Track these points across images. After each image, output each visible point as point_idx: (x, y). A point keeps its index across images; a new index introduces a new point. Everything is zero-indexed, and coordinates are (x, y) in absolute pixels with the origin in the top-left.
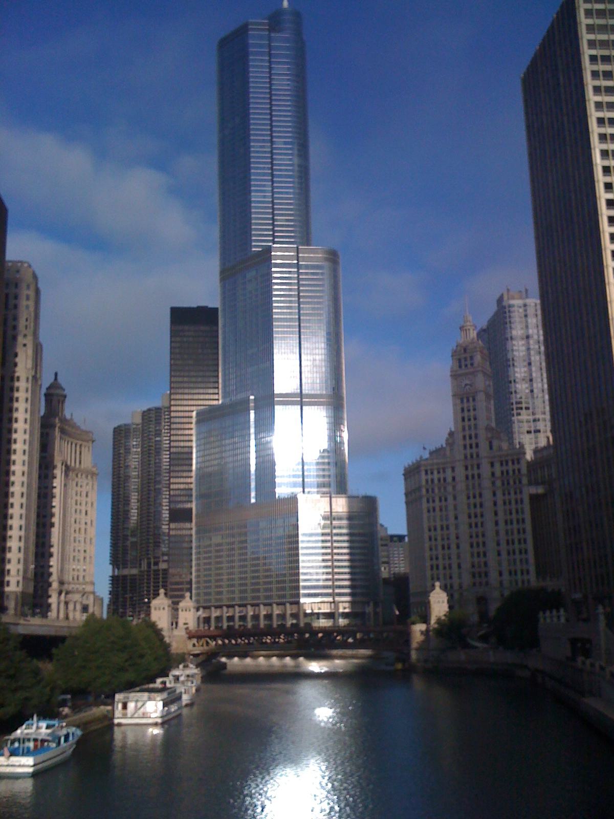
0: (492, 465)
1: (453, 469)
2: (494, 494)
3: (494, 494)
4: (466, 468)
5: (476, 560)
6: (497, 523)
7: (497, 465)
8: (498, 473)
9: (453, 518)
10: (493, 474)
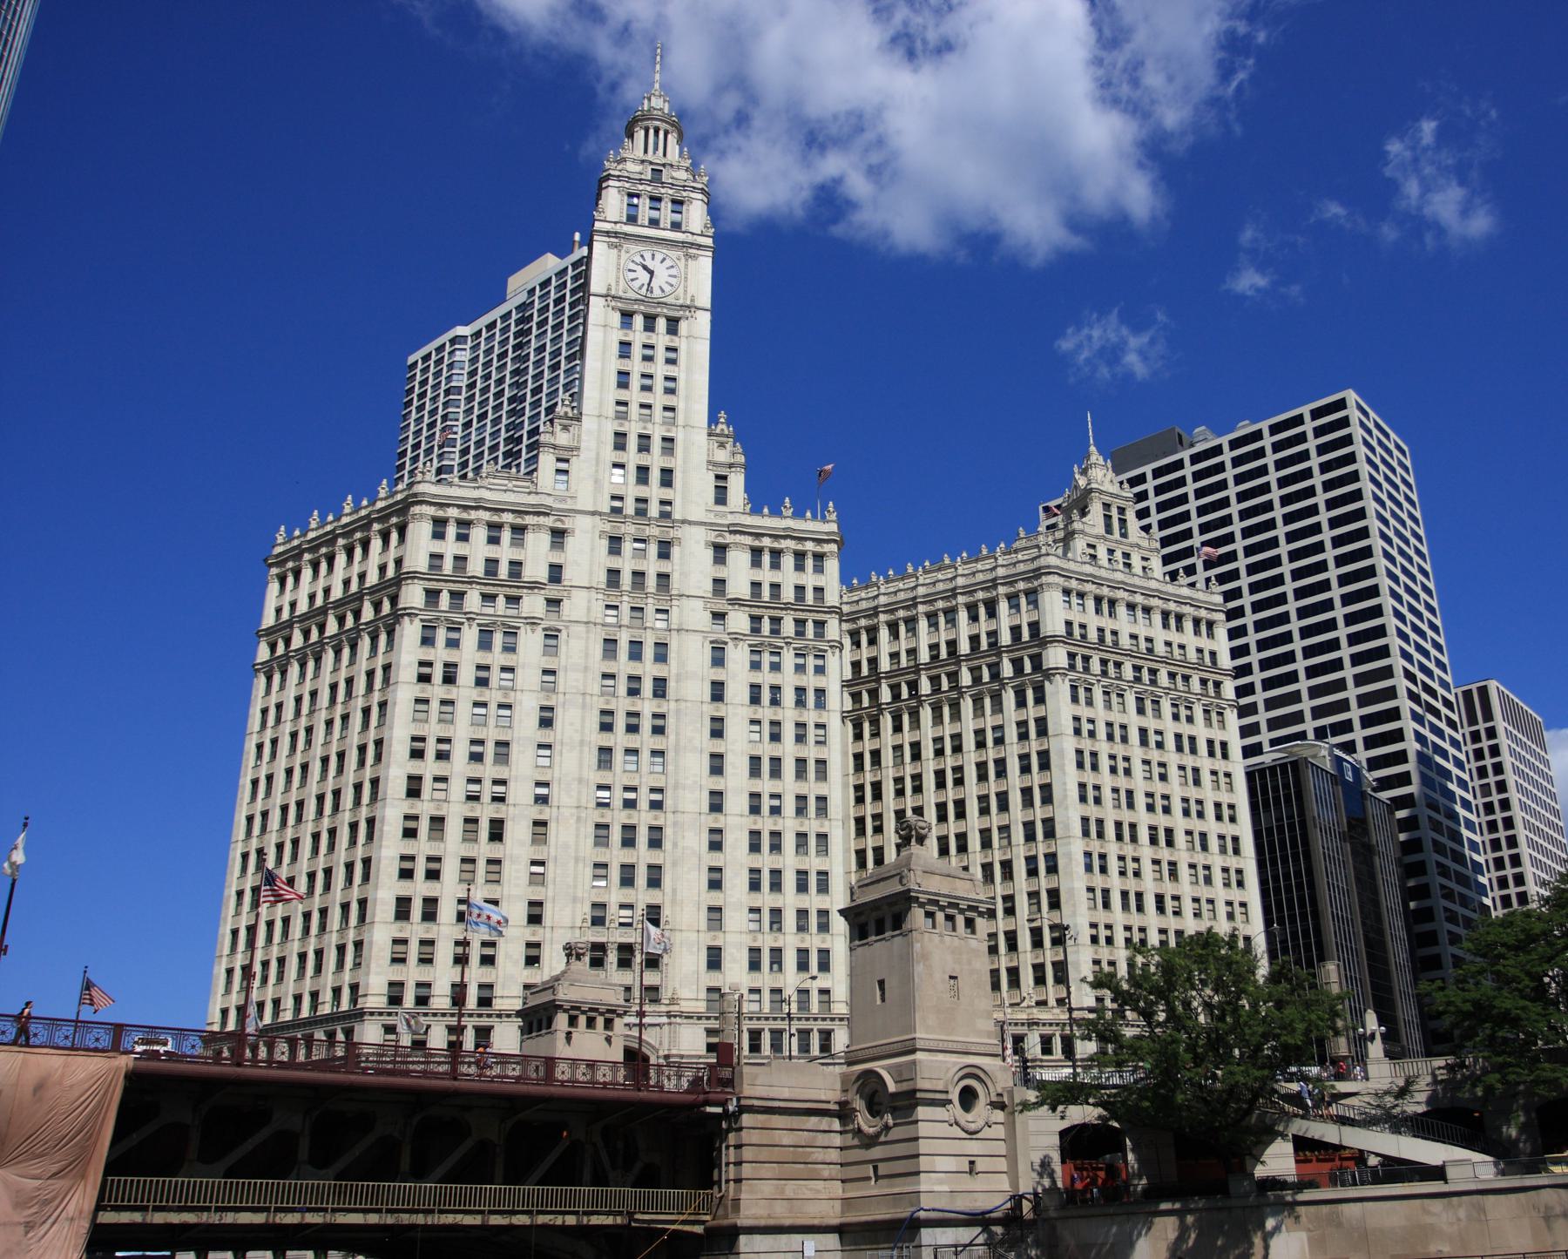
0: (720, 551)
2: (718, 660)
3: (718, 660)
4: (615, 544)
5: (615, 895)
6: (717, 764)
7: (739, 559)
8: (739, 586)
9: (534, 720)
10: (719, 583)
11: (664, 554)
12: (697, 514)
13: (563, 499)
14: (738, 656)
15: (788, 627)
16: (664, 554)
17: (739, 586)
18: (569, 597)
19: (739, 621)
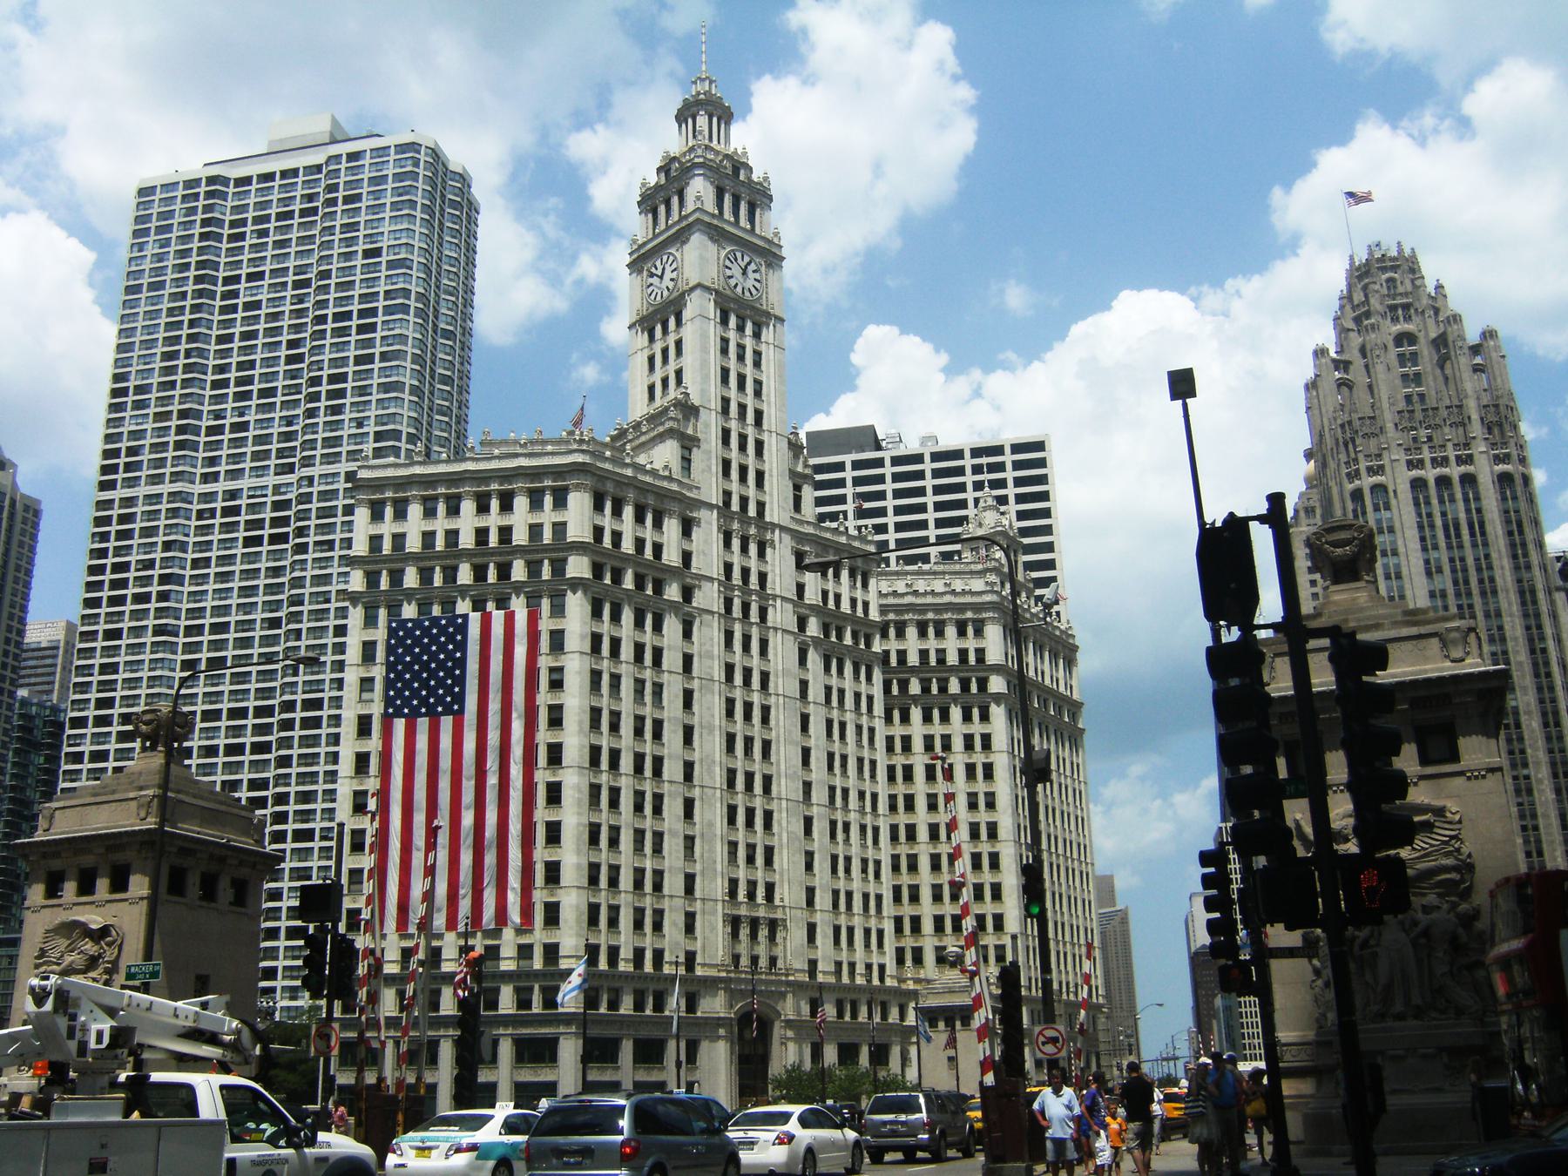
1: (687, 528)
2: (803, 661)
8: (812, 596)
11: (761, 554)
12: (786, 522)
13: (690, 488)
14: (813, 658)
15: (848, 640)
16: (761, 554)
17: (812, 596)
18: (700, 587)
19: (813, 628)
